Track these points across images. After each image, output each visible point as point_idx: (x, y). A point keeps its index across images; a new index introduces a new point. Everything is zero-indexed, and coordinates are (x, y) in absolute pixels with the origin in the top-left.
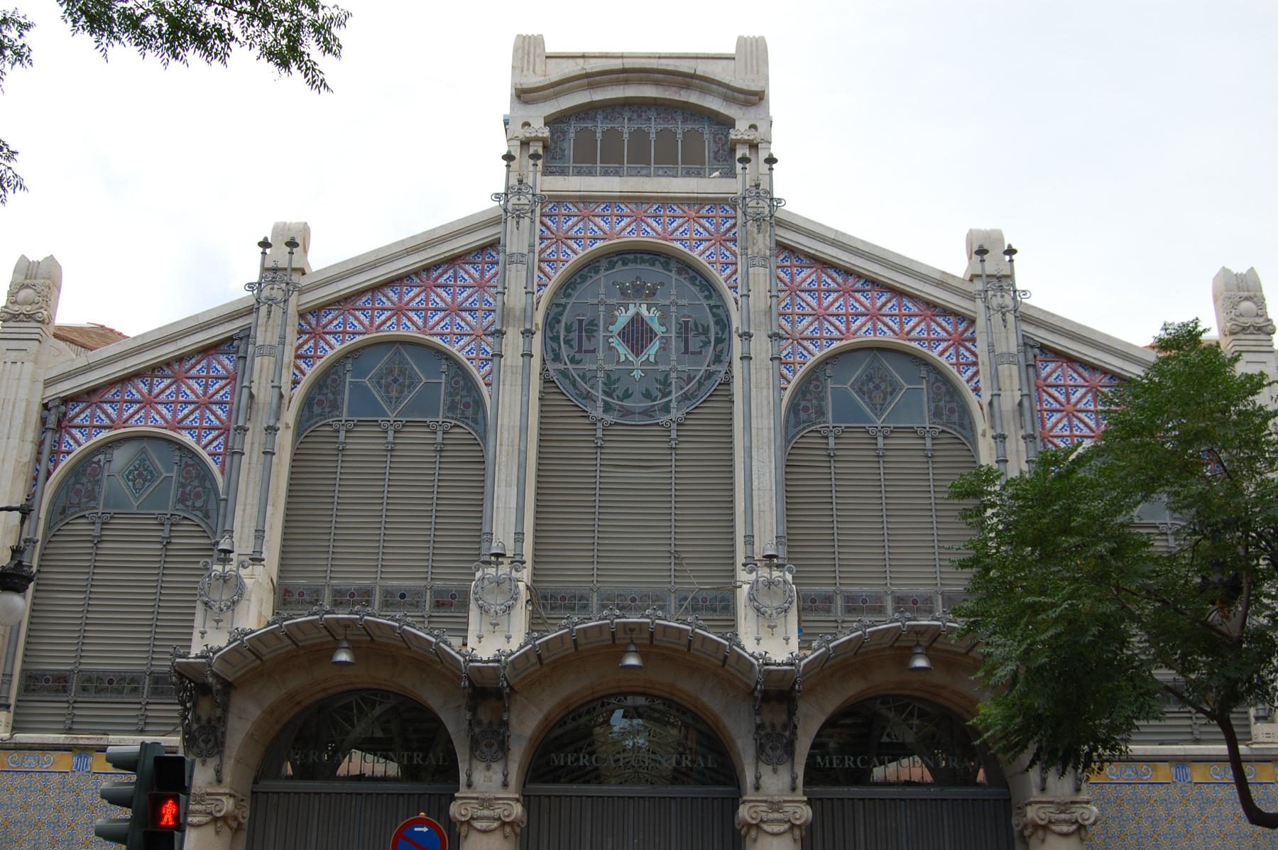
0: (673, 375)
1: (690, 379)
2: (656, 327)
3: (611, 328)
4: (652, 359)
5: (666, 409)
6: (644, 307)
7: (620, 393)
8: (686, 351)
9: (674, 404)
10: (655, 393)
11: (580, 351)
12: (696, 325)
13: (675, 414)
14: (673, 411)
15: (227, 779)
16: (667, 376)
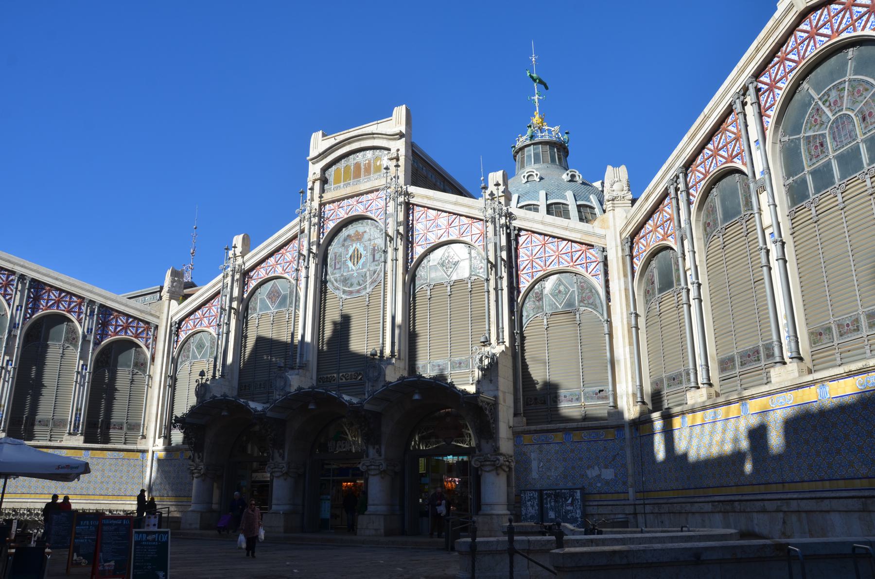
0: (368, 273)
1: (375, 272)
2: (364, 253)
3: (347, 256)
4: (361, 267)
5: (365, 288)
6: (358, 244)
7: (349, 285)
8: (374, 260)
9: (368, 286)
10: (361, 282)
11: (335, 269)
12: (378, 248)
13: (368, 290)
14: (368, 289)
15: (204, 461)
16: (365, 275)
